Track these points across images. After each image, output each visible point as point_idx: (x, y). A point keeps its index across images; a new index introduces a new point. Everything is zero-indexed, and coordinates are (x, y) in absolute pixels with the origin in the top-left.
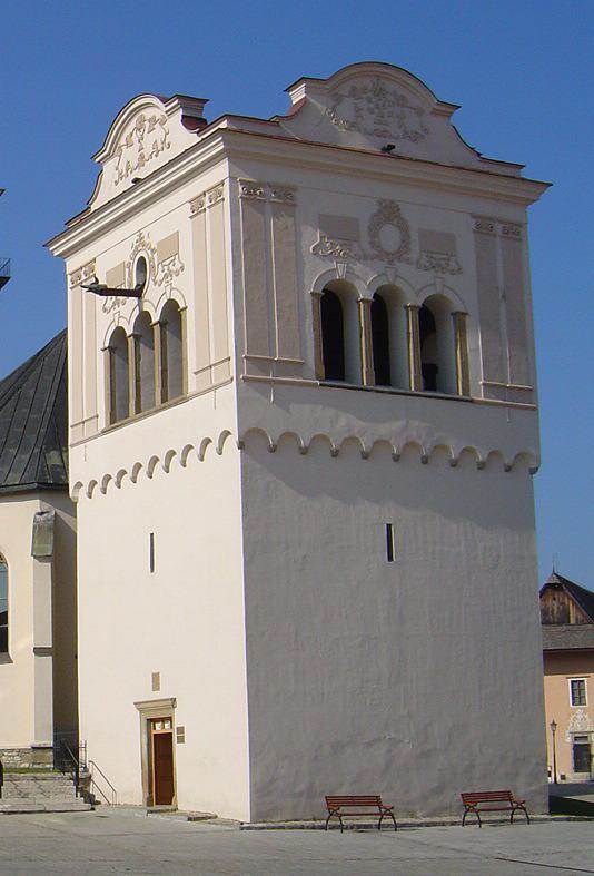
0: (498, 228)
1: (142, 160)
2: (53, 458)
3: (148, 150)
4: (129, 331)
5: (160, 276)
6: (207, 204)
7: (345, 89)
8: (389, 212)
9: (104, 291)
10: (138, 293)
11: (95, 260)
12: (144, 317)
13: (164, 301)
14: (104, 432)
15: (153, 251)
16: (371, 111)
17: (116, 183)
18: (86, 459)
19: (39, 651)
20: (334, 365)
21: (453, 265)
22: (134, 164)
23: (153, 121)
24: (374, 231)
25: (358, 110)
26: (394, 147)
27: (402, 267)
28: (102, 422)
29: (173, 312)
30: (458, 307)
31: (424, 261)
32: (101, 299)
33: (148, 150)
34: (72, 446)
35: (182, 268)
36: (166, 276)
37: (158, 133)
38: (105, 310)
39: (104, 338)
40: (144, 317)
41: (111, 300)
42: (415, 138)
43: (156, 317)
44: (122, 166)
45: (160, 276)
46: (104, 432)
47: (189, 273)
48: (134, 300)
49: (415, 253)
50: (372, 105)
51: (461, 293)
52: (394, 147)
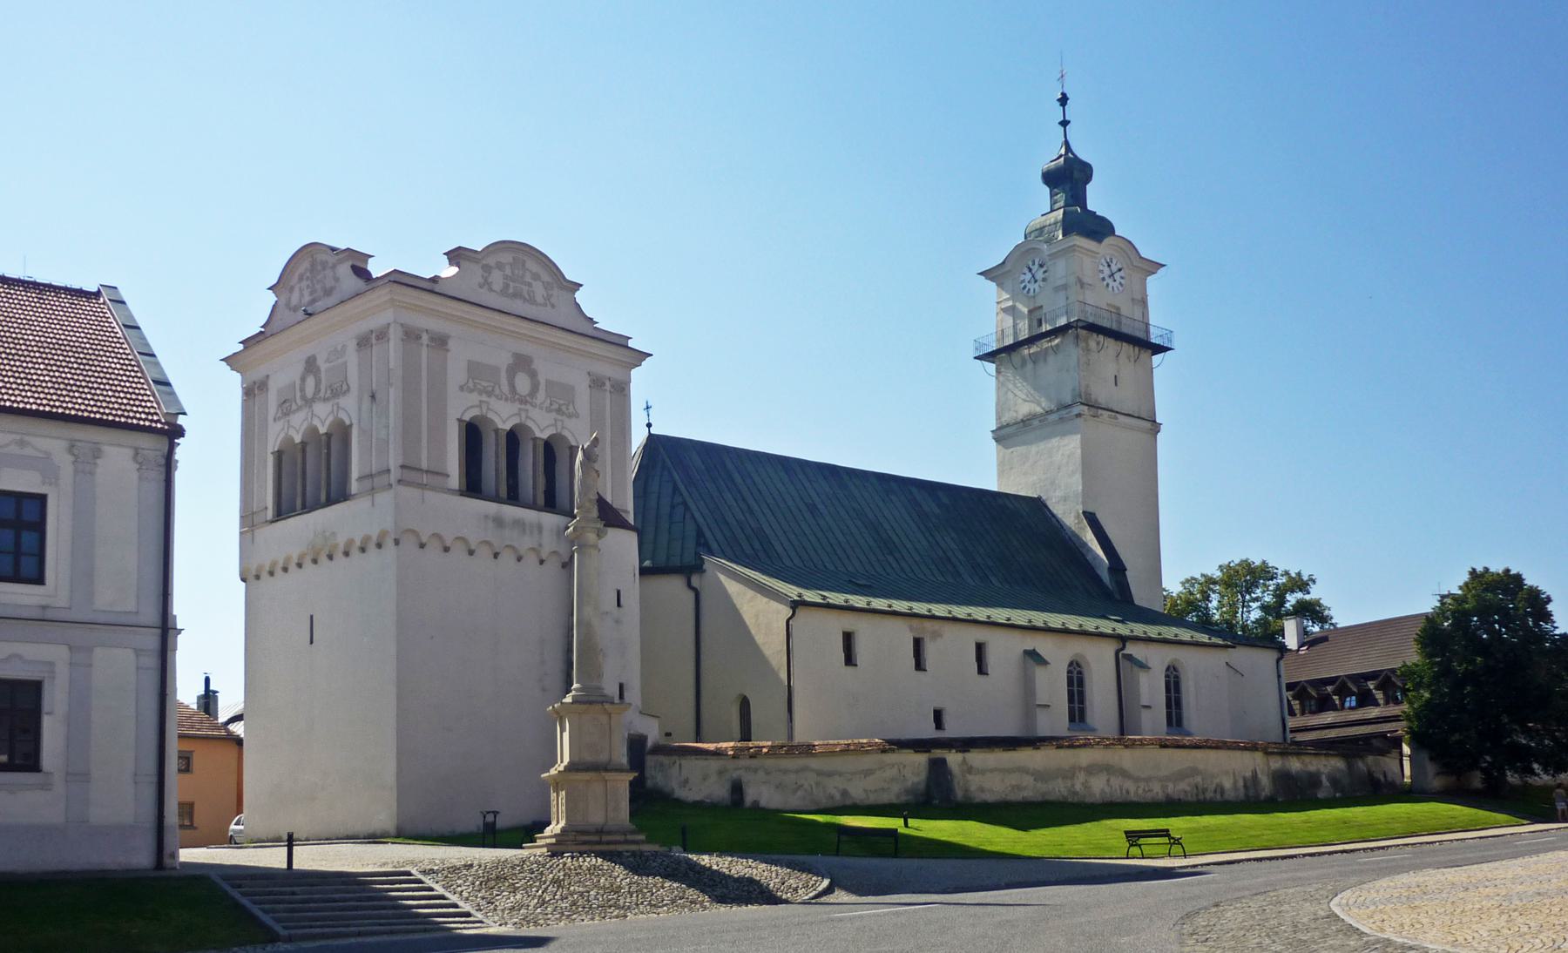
7: (491, 261)
8: (522, 363)
20: (473, 486)
24: (512, 372)
35: (348, 390)
51: (579, 434)
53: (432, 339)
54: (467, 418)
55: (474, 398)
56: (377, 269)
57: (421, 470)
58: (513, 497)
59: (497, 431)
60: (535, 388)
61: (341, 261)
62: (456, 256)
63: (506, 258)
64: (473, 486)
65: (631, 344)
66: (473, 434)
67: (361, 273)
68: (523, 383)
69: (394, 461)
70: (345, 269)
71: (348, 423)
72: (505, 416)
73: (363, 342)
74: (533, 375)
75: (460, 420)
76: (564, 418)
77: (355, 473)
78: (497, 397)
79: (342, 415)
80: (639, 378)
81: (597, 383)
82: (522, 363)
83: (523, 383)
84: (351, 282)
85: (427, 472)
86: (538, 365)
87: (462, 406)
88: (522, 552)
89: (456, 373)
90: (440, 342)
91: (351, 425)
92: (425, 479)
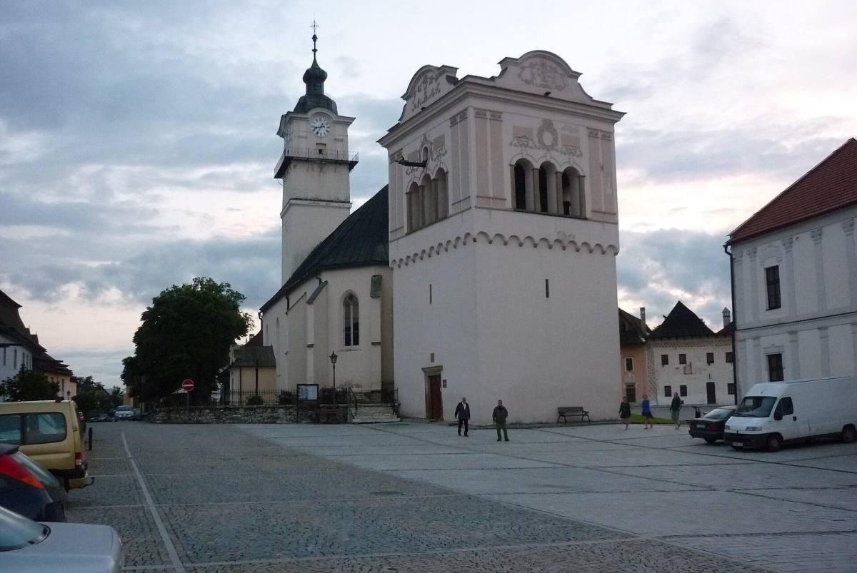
0: (600, 134)
1: (426, 99)
2: (380, 248)
3: (429, 93)
4: (419, 183)
5: (435, 156)
6: (458, 120)
7: (527, 63)
8: (548, 126)
9: (407, 164)
10: (424, 165)
11: (402, 149)
12: (427, 177)
13: (437, 169)
14: (407, 234)
15: (432, 144)
16: (539, 75)
17: (413, 110)
18: (398, 249)
19: (374, 344)
20: (520, 204)
21: (578, 153)
22: (422, 99)
23: (432, 79)
25: (533, 74)
26: (550, 93)
27: (554, 153)
28: (406, 230)
29: (442, 174)
30: (582, 174)
31: (564, 150)
32: (405, 168)
33: (429, 93)
34: (391, 242)
35: (446, 152)
36: (438, 156)
37: (434, 85)
38: (407, 173)
39: (406, 187)
40: (427, 177)
41: (410, 168)
42: (560, 88)
43: (432, 177)
44: (416, 101)
45: (435, 156)
46: (407, 234)
47: (449, 154)
48: (421, 168)
49: (560, 146)
50: (539, 72)
51: (583, 167)
52: (550, 93)
53: (493, 116)
54: (514, 163)
55: (518, 150)
56: (460, 75)
57: (489, 198)
58: (544, 210)
59: (534, 169)
60: (555, 139)
61: (440, 74)
62: (505, 63)
63: (537, 60)
64: (520, 204)
65: (613, 108)
66: (520, 170)
67: (452, 80)
68: (548, 138)
69: (474, 192)
70: (443, 79)
71: (446, 171)
72: (536, 158)
73: (453, 121)
74: (554, 133)
75: (511, 165)
76: (575, 157)
77: (451, 201)
78: (531, 147)
79: (442, 166)
80: (618, 128)
81: (593, 133)
82: (548, 126)
83: (548, 138)
84: (446, 87)
85: (493, 198)
86: (557, 126)
87: (511, 155)
88: (552, 243)
89: (507, 137)
90: (497, 116)
91: (447, 172)
92: (492, 203)
